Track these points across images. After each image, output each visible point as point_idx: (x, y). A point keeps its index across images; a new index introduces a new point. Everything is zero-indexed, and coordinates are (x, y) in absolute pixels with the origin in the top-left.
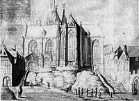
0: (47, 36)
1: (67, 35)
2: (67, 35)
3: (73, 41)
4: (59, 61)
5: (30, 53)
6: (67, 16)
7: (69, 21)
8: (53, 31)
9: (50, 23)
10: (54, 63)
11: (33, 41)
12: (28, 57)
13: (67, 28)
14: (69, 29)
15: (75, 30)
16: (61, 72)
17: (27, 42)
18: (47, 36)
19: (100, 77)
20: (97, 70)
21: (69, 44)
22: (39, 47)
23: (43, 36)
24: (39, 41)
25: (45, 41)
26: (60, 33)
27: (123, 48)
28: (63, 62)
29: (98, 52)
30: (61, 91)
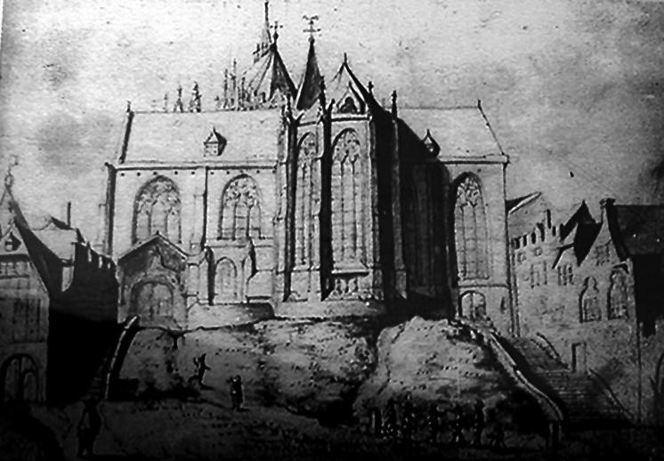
0: (229, 155)
1: (329, 149)
2: (329, 149)
3: (355, 189)
4: (287, 273)
5: (144, 238)
6: (327, 66)
7: (336, 92)
8: (258, 135)
9: (241, 97)
10: (261, 286)
11: (159, 183)
12: (135, 260)
13: (327, 121)
14: (336, 128)
15: (361, 127)
16: (300, 328)
17: (127, 186)
18: (229, 155)
19: (498, 348)
20: (479, 313)
21: (335, 192)
22: (191, 206)
23: (212, 159)
24: (190, 183)
25: (219, 179)
26: (295, 148)
27: (596, 212)
28: (306, 280)
29: (479, 233)
30: (299, 421)
